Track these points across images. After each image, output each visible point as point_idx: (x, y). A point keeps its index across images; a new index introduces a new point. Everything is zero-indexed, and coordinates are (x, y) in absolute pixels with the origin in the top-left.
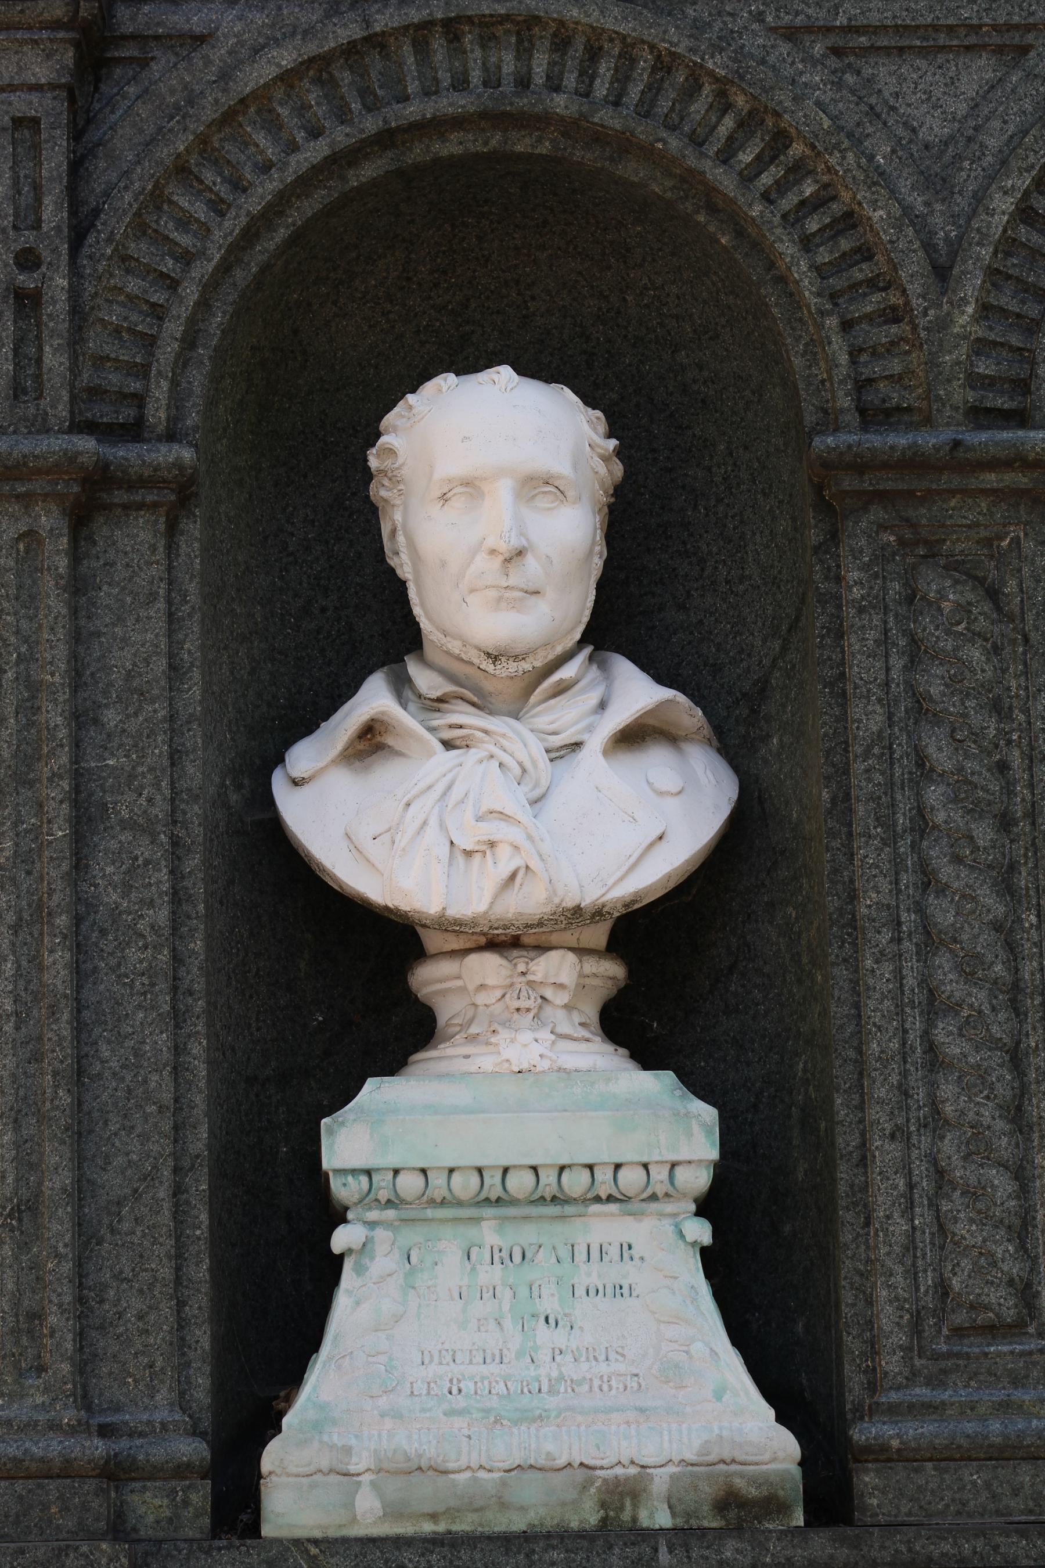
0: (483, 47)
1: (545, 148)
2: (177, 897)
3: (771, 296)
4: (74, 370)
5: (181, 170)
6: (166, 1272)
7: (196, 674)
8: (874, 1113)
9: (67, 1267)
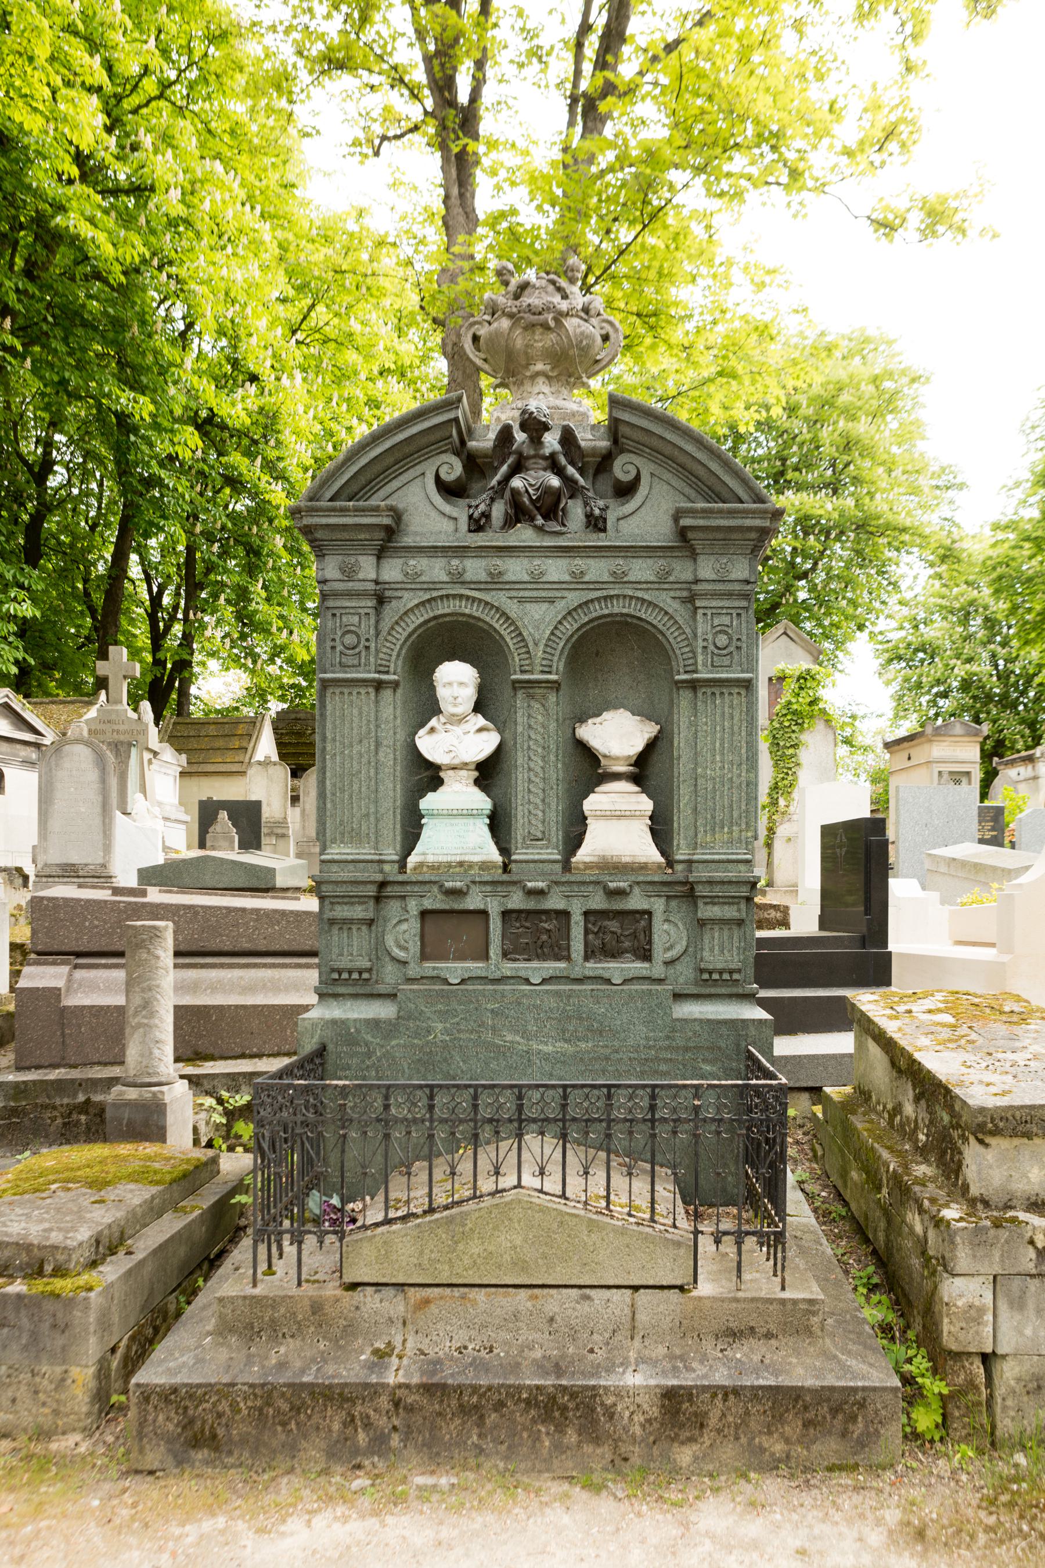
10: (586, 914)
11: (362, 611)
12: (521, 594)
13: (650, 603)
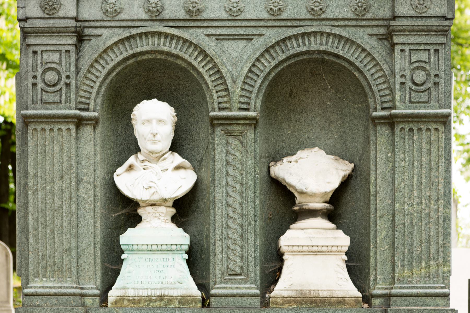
0: (152, 38)
1: (163, 57)
2: (95, 195)
3: (204, 86)
4: (76, 98)
5: (96, 61)
6: (92, 262)
7: (99, 155)
8: (217, 236)
9: (75, 260)
11: (63, 49)
12: (219, 31)
13: (347, 40)
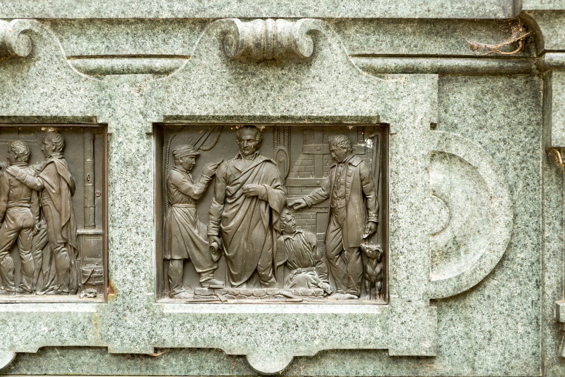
10: (163, 132)
